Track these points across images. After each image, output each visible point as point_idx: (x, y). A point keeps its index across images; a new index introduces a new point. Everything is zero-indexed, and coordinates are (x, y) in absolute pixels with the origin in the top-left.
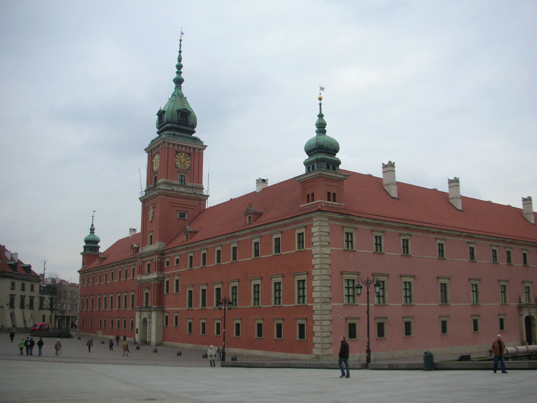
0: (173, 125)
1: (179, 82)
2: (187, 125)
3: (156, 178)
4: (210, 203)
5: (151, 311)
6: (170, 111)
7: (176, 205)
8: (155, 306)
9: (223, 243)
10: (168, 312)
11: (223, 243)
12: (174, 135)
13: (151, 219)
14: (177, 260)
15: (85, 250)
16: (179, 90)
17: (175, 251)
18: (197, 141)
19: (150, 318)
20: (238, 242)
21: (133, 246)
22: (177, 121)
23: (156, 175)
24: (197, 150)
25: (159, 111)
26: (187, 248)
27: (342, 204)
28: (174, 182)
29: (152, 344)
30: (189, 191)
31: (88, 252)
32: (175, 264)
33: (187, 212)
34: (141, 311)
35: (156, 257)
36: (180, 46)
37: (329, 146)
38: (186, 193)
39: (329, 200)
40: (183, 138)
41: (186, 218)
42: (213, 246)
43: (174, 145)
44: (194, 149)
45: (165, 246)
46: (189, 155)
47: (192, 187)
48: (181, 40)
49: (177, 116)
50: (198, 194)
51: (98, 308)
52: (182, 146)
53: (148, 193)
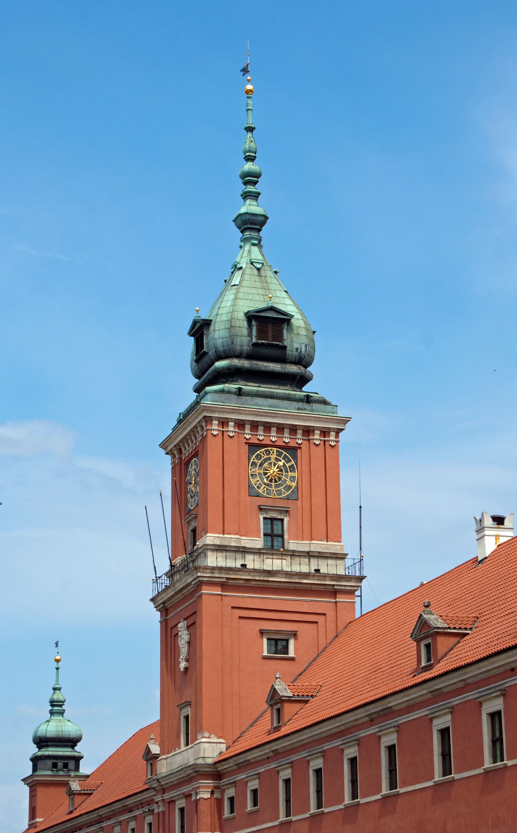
0: (236, 362)
2: (283, 360)
3: (194, 531)
6: (224, 318)
9: (363, 734)
11: (363, 734)
12: (240, 392)
13: (183, 665)
15: (35, 769)
18: (316, 406)
20: (399, 729)
21: (148, 750)
22: (246, 348)
23: (193, 524)
24: (317, 435)
25: (195, 322)
26: (277, 755)
28: (247, 542)
30: (296, 568)
31: (45, 773)
32: (250, 807)
33: (295, 635)
38: (288, 574)
40: (271, 401)
41: (292, 653)
42: (337, 743)
43: (240, 425)
44: (308, 431)
45: (223, 747)
46: (293, 450)
47: (309, 555)
49: (245, 332)
50: (325, 576)
52: (267, 427)
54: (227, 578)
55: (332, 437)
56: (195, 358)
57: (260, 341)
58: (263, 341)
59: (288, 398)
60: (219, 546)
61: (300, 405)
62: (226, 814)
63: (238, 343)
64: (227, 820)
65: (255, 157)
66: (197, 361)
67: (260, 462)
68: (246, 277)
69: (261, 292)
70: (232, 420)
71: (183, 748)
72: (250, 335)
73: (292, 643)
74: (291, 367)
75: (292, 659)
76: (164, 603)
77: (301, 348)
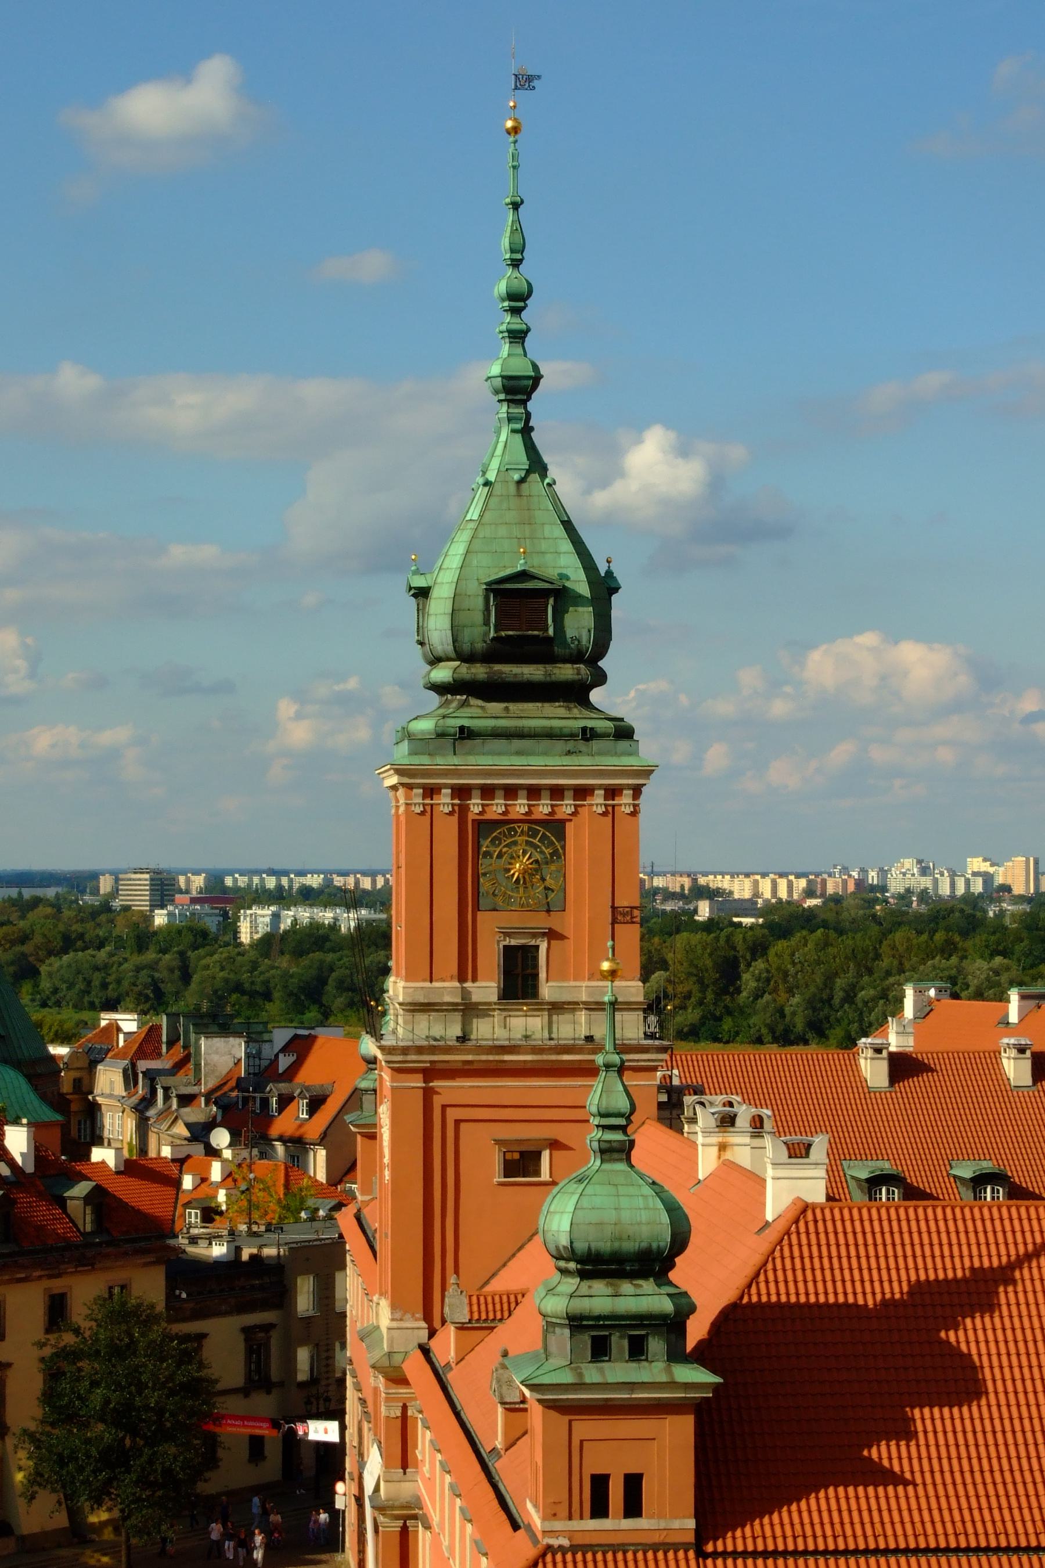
16: (518, 438)
22: (480, 646)
24: (598, 799)
27: (676, 1524)
37: (605, 1246)
39: (600, 1510)
41: (545, 1175)
43: (462, 792)
44: (582, 793)
49: (479, 618)
55: (626, 799)
57: (503, 634)
58: (511, 633)
59: (550, 735)
60: (422, 1004)
61: (571, 745)
63: (466, 639)
65: (521, 261)
67: (498, 850)
68: (494, 501)
69: (516, 531)
70: (446, 786)
72: (486, 623)
73: (546, 1155)
74: (563, 671)
77: (581, 636)
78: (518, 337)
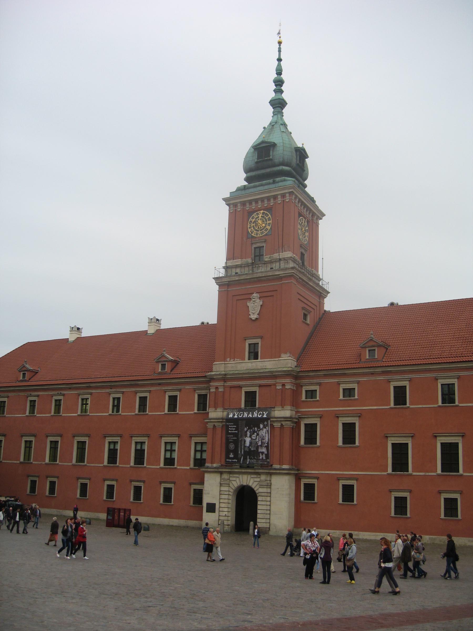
1: (278, 104)
2: (301, 176)
4: (332, 305)
5: (271, 474)
7: (303, 299)
8: (285, 467)
10: (318, 478)
12: (299, 186)
13: (253, 317)
14: (349, 392)
17: (344, 375)
19: (269, 486)
25: (263, 142)
29: (271, 533)
32: (341, 397)
34: (230, 473)
35: (288, 380)
36: (280, 51)
41: (308, 321)
44: (313, 214)
48: (280, 43)
49: (295, 157)
51: (22, 460)
53: (238, 270)
54: (300, 278)
56: (256, 160)
62: (304, 398)
64: (303, 401)
66: (257, 163)
71: (247, 360)
75: (308, 325)
76: (229, 281)
78: (282, 92)
